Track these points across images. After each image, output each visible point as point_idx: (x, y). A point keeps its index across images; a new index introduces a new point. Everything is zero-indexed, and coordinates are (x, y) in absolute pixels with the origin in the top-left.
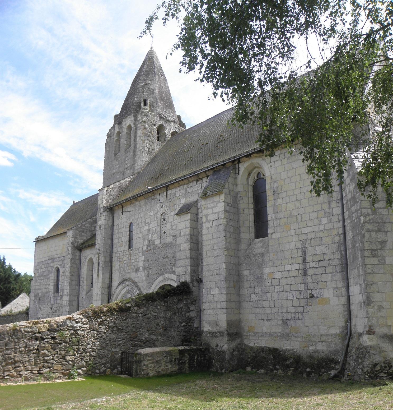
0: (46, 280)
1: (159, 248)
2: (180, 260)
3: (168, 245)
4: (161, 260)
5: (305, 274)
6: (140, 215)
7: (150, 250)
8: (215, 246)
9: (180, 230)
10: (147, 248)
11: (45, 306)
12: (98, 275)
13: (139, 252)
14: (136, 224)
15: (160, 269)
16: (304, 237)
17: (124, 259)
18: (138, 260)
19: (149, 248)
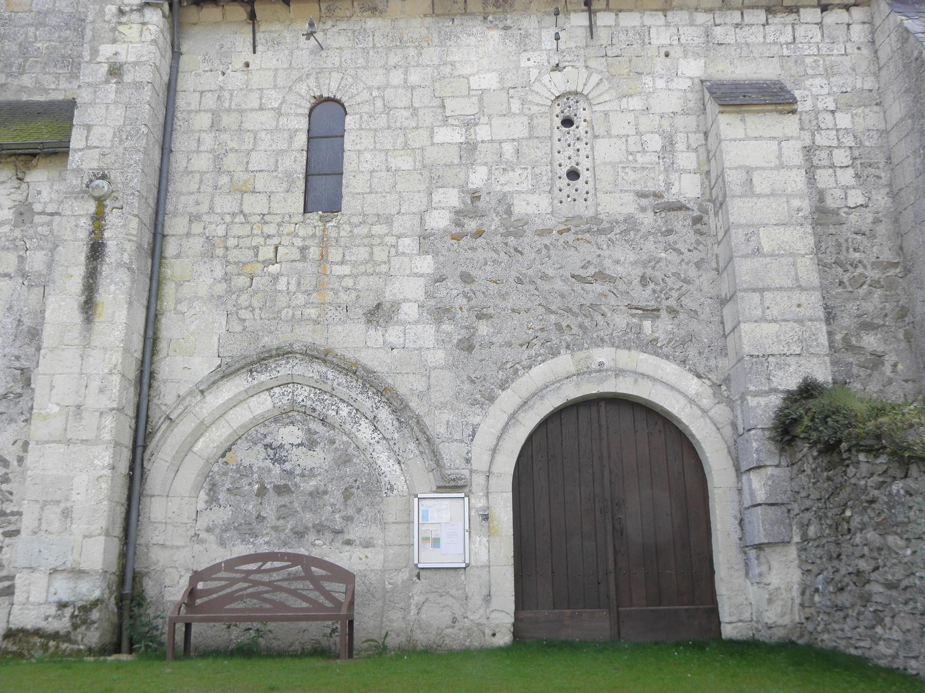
1: (541, 233)
4: (559, 285)
7: (479, 234)
9: (749, 171)
10: (458, 224)
12: (89, 306)
19: (472, 225)
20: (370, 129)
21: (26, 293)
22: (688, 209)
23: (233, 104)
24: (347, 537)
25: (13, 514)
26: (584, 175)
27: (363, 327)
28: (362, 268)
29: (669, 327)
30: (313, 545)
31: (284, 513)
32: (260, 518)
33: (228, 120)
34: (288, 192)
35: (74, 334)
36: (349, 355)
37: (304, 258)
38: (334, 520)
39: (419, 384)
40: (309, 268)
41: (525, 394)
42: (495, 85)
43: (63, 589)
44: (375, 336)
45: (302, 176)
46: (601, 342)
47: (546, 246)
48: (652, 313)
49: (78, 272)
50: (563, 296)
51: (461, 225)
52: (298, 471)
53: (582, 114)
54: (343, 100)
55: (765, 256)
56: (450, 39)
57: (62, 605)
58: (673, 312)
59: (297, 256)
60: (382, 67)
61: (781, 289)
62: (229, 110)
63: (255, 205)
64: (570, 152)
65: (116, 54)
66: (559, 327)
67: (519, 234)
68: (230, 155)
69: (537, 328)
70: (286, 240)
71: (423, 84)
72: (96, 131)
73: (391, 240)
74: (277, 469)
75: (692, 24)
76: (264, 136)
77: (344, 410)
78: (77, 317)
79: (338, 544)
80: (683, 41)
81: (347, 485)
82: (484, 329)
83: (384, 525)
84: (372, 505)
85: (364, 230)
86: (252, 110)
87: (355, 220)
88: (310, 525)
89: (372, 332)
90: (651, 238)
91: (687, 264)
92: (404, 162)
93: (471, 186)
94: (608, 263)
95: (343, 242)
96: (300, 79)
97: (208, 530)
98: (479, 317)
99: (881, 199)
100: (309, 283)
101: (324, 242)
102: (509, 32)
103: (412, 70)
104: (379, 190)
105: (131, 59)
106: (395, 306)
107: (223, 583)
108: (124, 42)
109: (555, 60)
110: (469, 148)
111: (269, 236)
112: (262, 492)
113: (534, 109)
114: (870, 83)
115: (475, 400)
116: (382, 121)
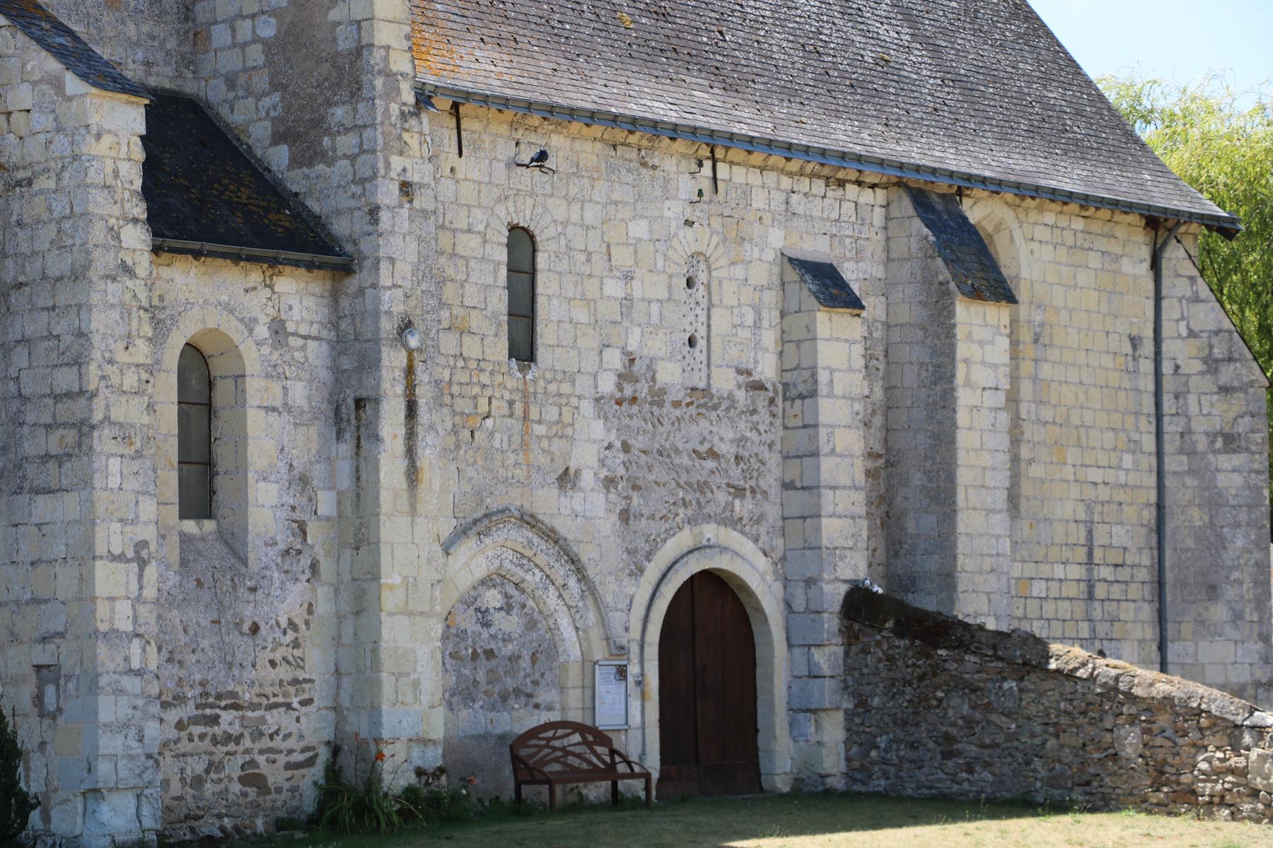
1: (676, 404)
2: (834, 488)
3: (716, 400)
4: (685, 460)
5: (1091, 596)
6: (576, 207)
8: (988, 474)
10: (620, 388)
13: (578, 391)
14: (553, 246)
15: (683, 499)
16: (1090, 493)
17: (483, 407)
18: (569, 431)
19: (628, 391)
20: (556, 272)
21: (293, 432)
22: (766, 389)
23: (447, 219)
24: (535, 700)
25: (306, 681)
26: (701, 344)
27: (556, 491)
29: (751, 506)
30: (513, 708)
32: (476, 683)
34: (496, 336)
35: (404, 503)
37: (511, 415)
38: (526, 685)
39: (595, 554)
42: (646, 236)
45: (506, 318)
47: (678, 419)
52: (500, 636)
54: (536, 232)
55: (837, 455)
56: (613, 172)
58: (753, 491)
59: (506, 411)
60: (565, 198)
61: (844, 487)
63: (472, 348)
64: (692, 318)
67: (660, 404)
68: (449, 284)
69: (672, 501)
71: (595, 225)
72: (399, 265)
74: (485, 635)
76: (473, 266)
79: (530, 708)
80: (772, 207)
81: (534, 650)
83: (562, 689)
85: (553, 388)
86: (462, 231)
87: (549, 375)
88: (511, 689)
89: (563, 498)
90: (743, 417)
91: (764, 444)
92: (581, 315)
93: (630, 349)
94: (716, 440)
95: (539, 396)
96: (499, 200)
98: (636, 488)
102: (657, 172)
103: (587, 205)
104: (565, 344)
106: (578, 472)
107: (533, 750)
108: (409, 156)
111: (484, 386)
112: (475, 656)
115: (631, 570)
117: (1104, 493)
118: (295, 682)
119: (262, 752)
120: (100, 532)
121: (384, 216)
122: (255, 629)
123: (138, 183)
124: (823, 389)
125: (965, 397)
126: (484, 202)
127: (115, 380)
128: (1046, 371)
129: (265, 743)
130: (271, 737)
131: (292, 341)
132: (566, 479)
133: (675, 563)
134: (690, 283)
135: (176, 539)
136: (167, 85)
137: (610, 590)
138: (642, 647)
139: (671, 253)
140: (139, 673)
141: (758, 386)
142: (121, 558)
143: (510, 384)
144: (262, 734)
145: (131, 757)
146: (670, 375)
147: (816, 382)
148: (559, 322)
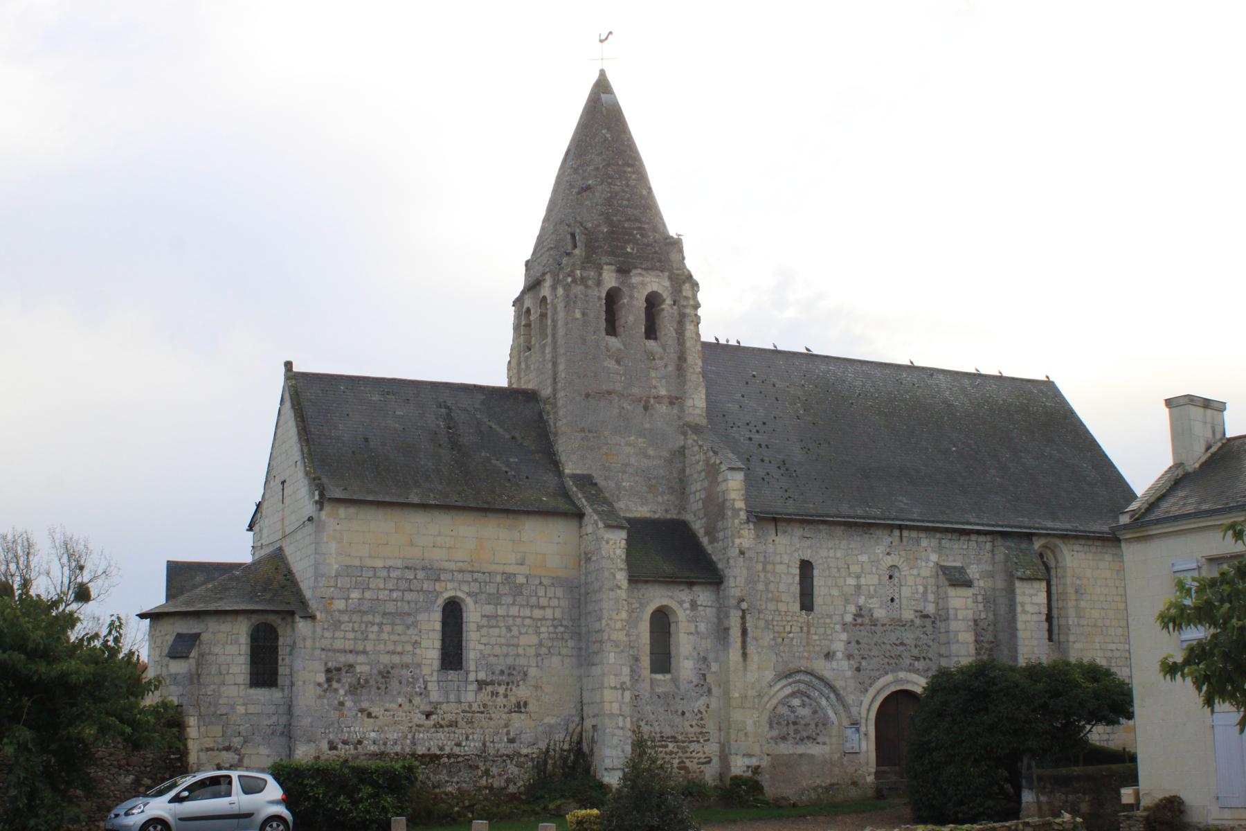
0: (399, 629)
1: (883, 625)
7: (861, 625)
8: (1036, 649)
9: (956, 610)
11: (393, 706)
13: (834, 621)
16: (1110, 654)
17: (788, 629)
26: (897, 601)
27: (823, 661)
28: (822, 637)
31: (796, 732)
32: (788, 734)
33: (769, 567)
36: (820, 672)
40: (804, 635)
41: (878, 689)
43: (747, 761)
44: (828, 665)
46: (901, 669)
48: (917, 659)
49: (739, 640)
50: (890, 651)
51: (855, 620)
53: (897, 574)
57: (748, 767)
58: (924, 658)
59: (799, 630)
62: (769, 562)
63: (783, 607)
65: (741, 543)
66: (888, 663)
67: (875, 625)
70: (795, 623)
72: (738, 579)
73: (832, 625)
74: (792, 715)
75: (934, 538)
77: (817, 693)
78: (741, 659)
82: (864, 663)
84: (825, 729)
86: (778, 563)
87: (819, 616)
92: (835, 592)
96: (795, 551)
97: (772, 738)
98: (863, 658)
99: (991, 616)
100: (804, 643)
101: (809, 626)
105: (747, 546)
106: (834, 653)
109: (888, 550)
110: (858, 587)
111: (788, 622)
112: (788, 724)
113: (881, 572)
114: (990, 568)
116: (827, 573)
117: (1117, 654)
118: (701, 733)
119: (687, 758)
120: (606, 680)
121: (732, 562)
122: (683, 713)
123: (624, 557)
124: (952, 616)
125: (1021, 618)
126: (788, 552)
127: (613, 625)
128: (1083, 604)
129: (688, 755)
130: (691, 753)
131: (700, 608)
132: (829, 656)
133: (884, 687)
134: (891, 577)
135: (649, 681)
136: (675, 517)
137: (850, 699)
138: (867, 720)
139: (880, 567)
140: (622, 728)
141: (927, 616)
142: (615, 688)
143: (800, 620)
144: (687, 752)
145: (619, 758)
146: (880, 613)
147: (948, 615)
148: (825, 595)
